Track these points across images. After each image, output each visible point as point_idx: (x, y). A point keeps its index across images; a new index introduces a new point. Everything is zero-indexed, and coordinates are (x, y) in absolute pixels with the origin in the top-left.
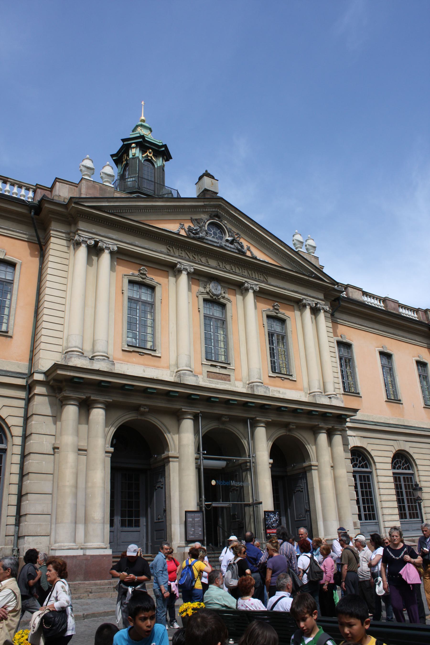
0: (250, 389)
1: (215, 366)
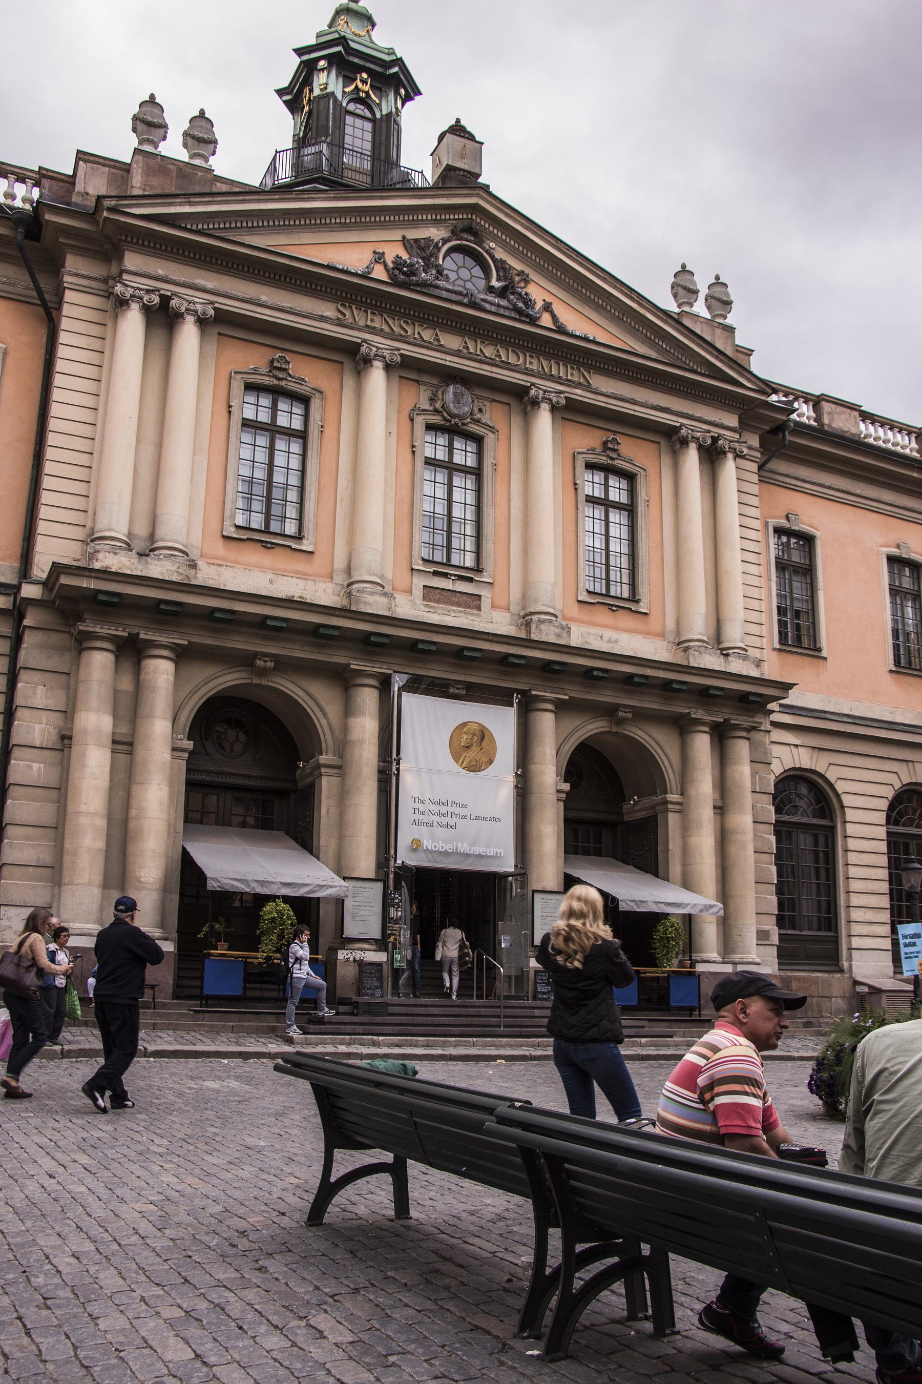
0: (523, 627)
1: (446, 575)
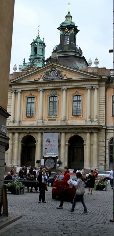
1: (51, 117)
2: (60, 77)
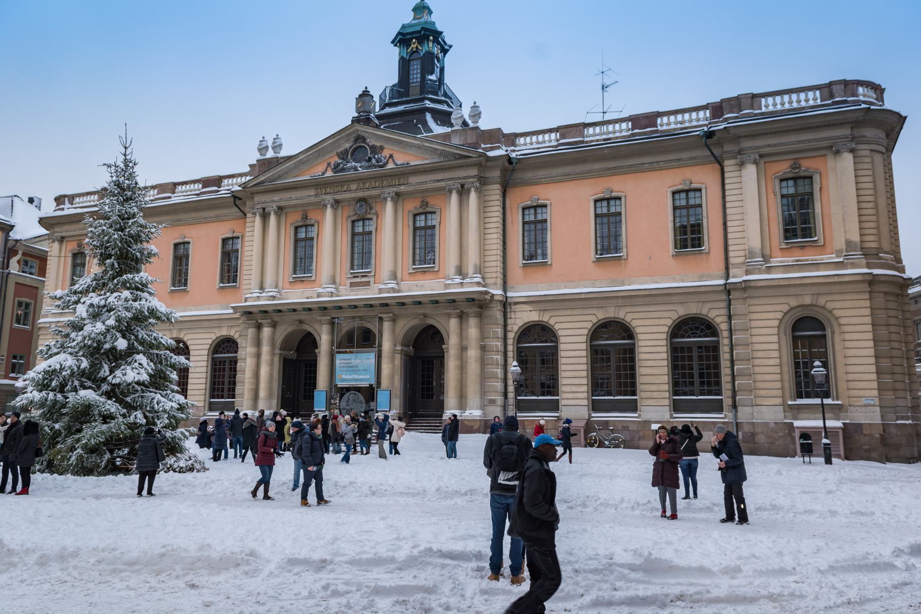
2: (377, 162)
